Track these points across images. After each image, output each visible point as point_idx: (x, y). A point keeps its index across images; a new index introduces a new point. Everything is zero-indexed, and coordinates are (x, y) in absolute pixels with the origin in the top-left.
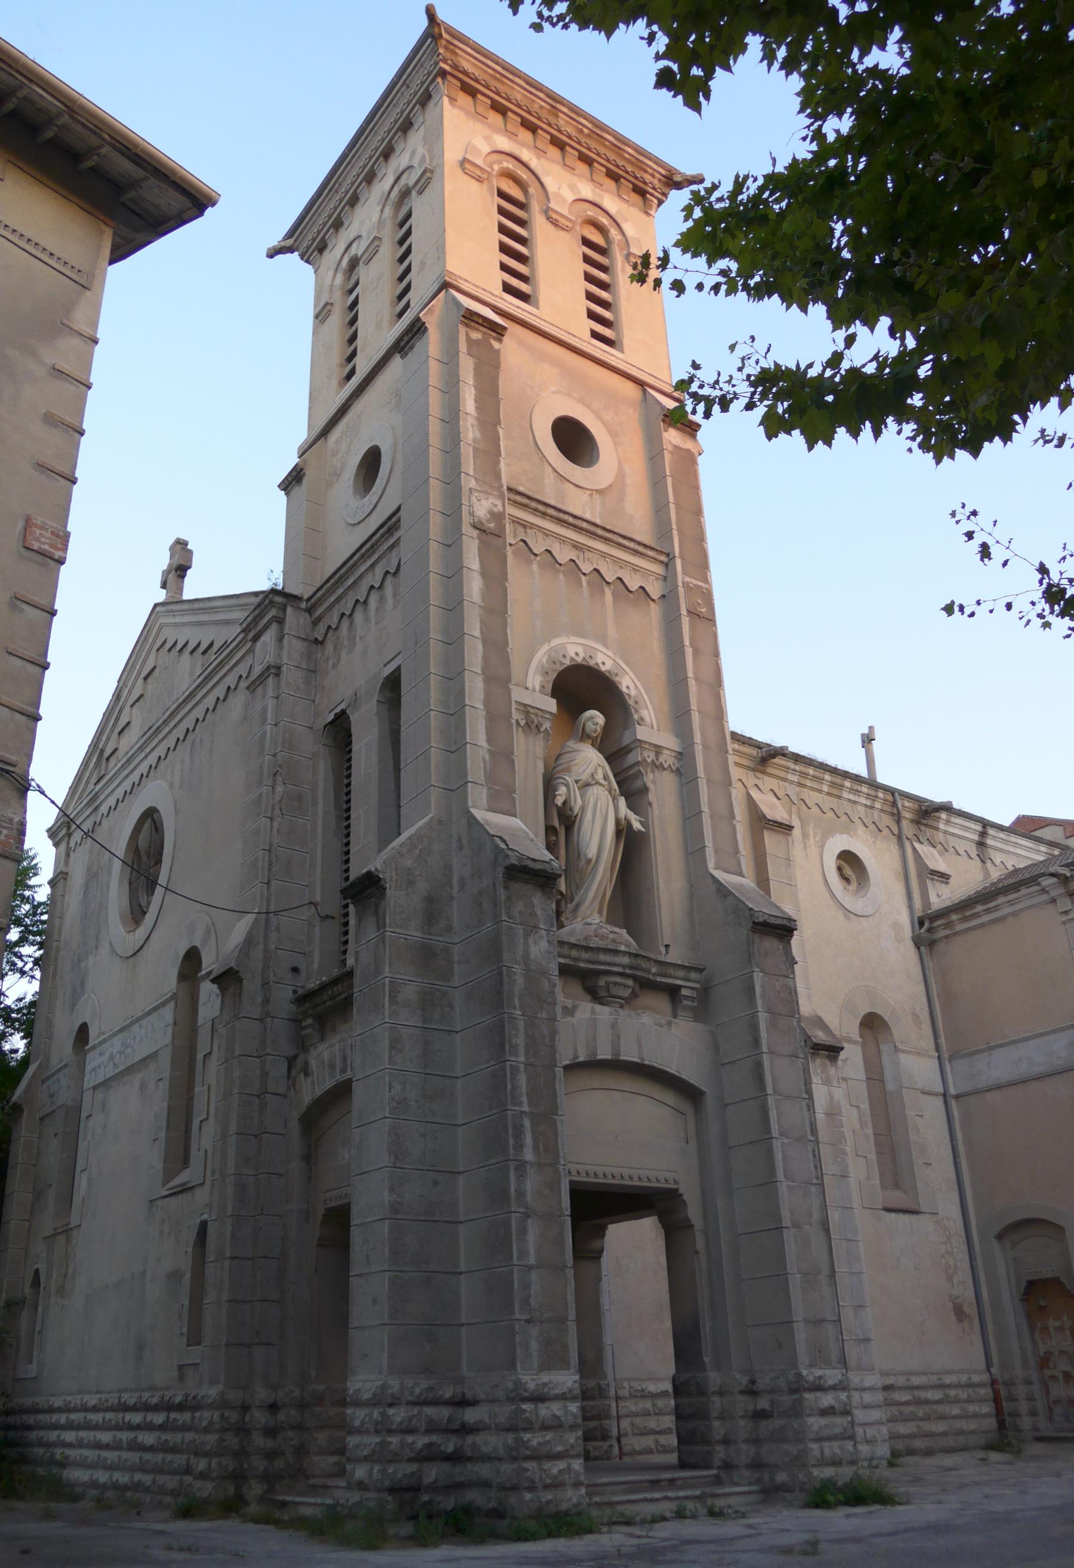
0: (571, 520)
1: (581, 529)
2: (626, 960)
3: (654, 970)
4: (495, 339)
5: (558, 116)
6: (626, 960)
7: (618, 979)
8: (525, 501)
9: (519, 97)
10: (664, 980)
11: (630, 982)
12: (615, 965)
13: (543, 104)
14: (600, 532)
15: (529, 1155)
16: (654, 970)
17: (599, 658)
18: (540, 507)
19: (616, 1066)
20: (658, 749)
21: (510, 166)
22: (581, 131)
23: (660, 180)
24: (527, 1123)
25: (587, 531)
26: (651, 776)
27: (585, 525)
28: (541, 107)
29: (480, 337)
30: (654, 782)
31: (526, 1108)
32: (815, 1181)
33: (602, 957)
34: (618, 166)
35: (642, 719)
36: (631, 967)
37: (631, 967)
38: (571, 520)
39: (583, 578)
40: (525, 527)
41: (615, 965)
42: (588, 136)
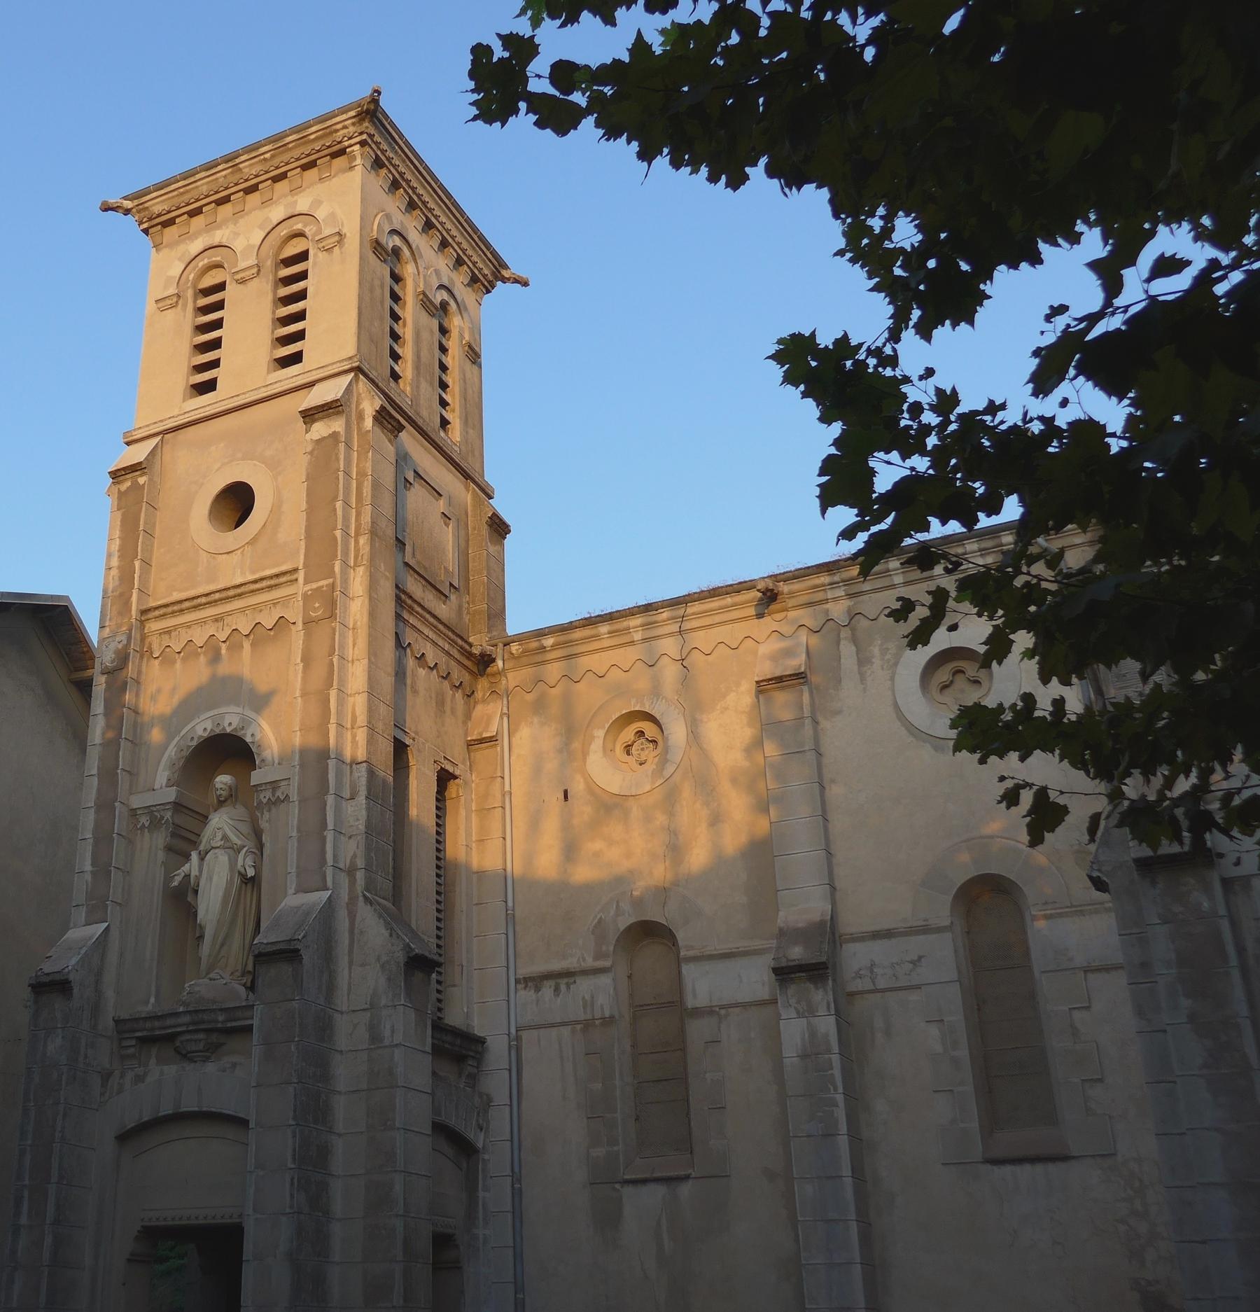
0: (203, 600)
1: (216, 601)
2: (187, 1019)
3: (221, 1018)
4: (141, 475)
5: (240, 169)
6: (187, 1019)
7: (188, 1037)
8: (162, 611)
9: (204, 190)
10: (234, 1024)
11: (201, 1036)
12: (180, 1025)
13: (224, 173)
14: (231, 593)
15: (24, 1220)
16: (221, 1018)
17: (200, 732)
18: (175, 608)
19: (179, 1118)
20: (274, 785)
21: (206, 261)
22: (265, 159)
23: (353, 124)
24: (26, 1194)
25: (221, 600)
26: (267, 815)
27: (217, 596)
28: (225, 177)
29: (128, 484)
30: (269, 821)
31: (27, 1182)
32: (288, 1210)
33: (169, 1022)
34: (308, 155)
35: (263, 760)
36: (194, 1023)
37: (194, 1023)
38: (203, 600)
39: (223, 645)
40: (169, 632)
41: (180, 1025)
42: (273, 157)
